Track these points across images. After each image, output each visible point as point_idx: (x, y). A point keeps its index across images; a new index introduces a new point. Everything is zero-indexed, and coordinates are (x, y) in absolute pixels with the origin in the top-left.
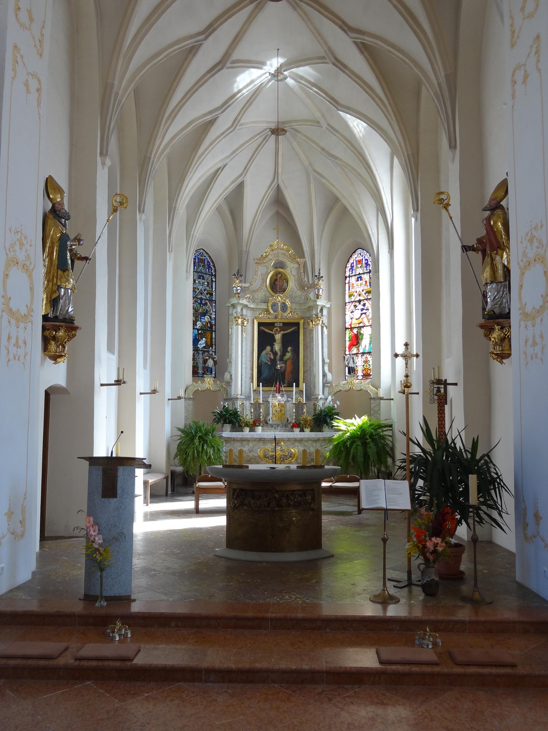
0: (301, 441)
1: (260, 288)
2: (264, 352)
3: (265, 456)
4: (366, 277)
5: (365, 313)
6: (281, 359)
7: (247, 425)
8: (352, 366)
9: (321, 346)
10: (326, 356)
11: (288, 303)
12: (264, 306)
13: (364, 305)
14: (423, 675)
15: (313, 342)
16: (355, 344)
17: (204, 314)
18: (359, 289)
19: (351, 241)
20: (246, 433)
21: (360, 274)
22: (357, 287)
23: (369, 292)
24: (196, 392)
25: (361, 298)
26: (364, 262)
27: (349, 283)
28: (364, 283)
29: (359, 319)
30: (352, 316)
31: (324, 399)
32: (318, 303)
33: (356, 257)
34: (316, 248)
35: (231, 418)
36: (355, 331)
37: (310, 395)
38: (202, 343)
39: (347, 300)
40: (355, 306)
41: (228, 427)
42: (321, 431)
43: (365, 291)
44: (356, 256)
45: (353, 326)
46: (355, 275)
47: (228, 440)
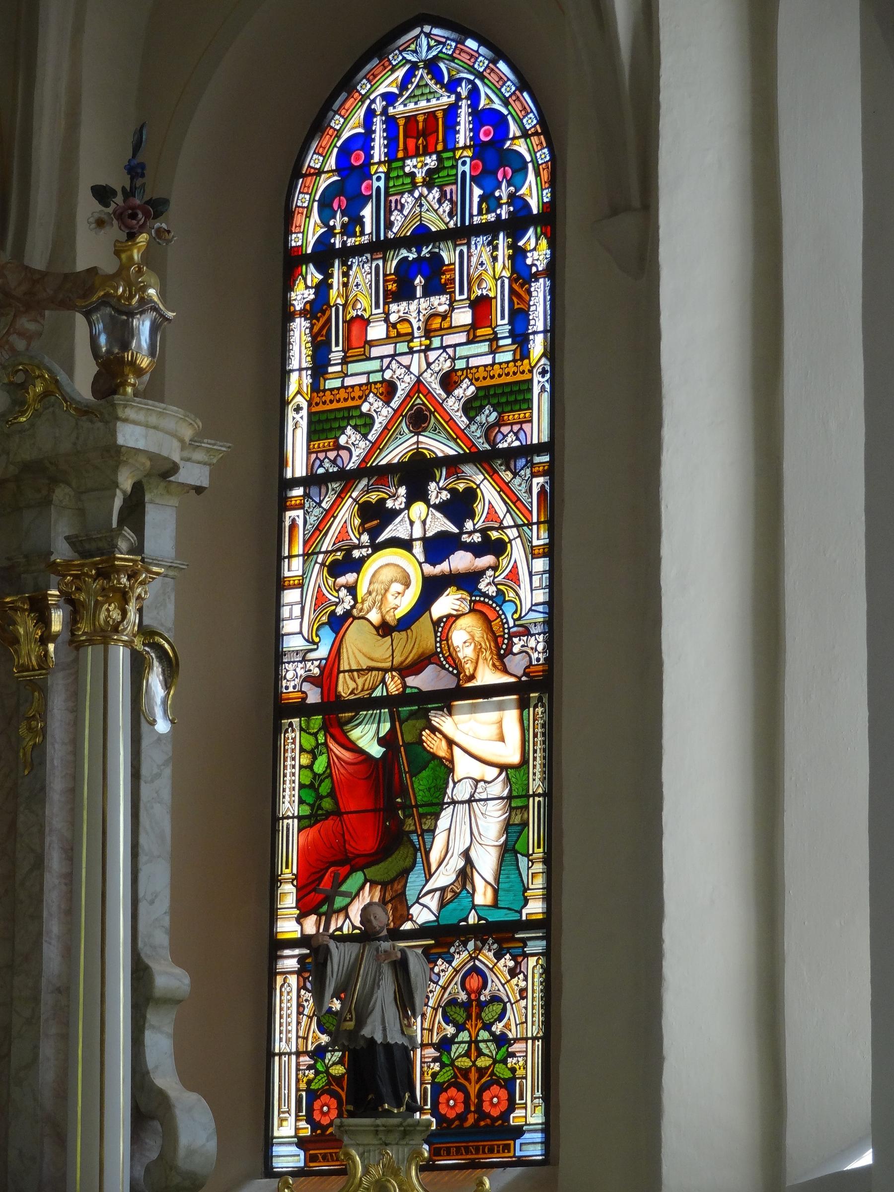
5: (467, 581)
8: (395, 1038)
10: (161, 938)
13: (460, 506)
15: (40, 793)
16: (367, 843)
18: (412, 369)
21: (422, 235)
23: (509, 397)
25: (438, 446)
26: (463, 137)
27: (318, 308)
28: (463, 317)
29: (407, 622)
30: (355, 598)
32: (129, 436)
36: (367, 737)
40: (375, 516)
43: (465, 390)
44: (389, 84)
45: (345, 687)
46: (379, 247)
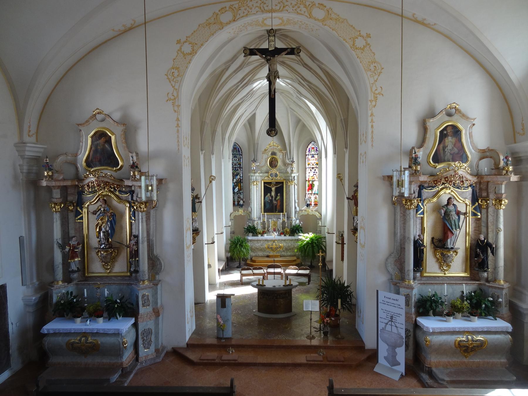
0: (285, 240)
1: (264, 165)
2: (267, 196)
3: (268, 248)
4: (316, 156)
6: (275, 200)
7: (260, 233)
9: (294, 194)
11: (278, 173)
12: (267, 175)
14: (318, 364)
17: (237, 175)
18: (313, 162)
19: (308, 139)
20: (260, 237)
22: (312, 161)
23: (317, 164)
24: (235, 217)
30: (309, 175)
31: (295, 221)
33: (311, 146)
34: (291, 141)
35: (252, 230)
37: (289, 217)
38: (236, 190)
39: (307, 166)
41: (251, 234)
42: (294, 236)
47: (251, 241)
